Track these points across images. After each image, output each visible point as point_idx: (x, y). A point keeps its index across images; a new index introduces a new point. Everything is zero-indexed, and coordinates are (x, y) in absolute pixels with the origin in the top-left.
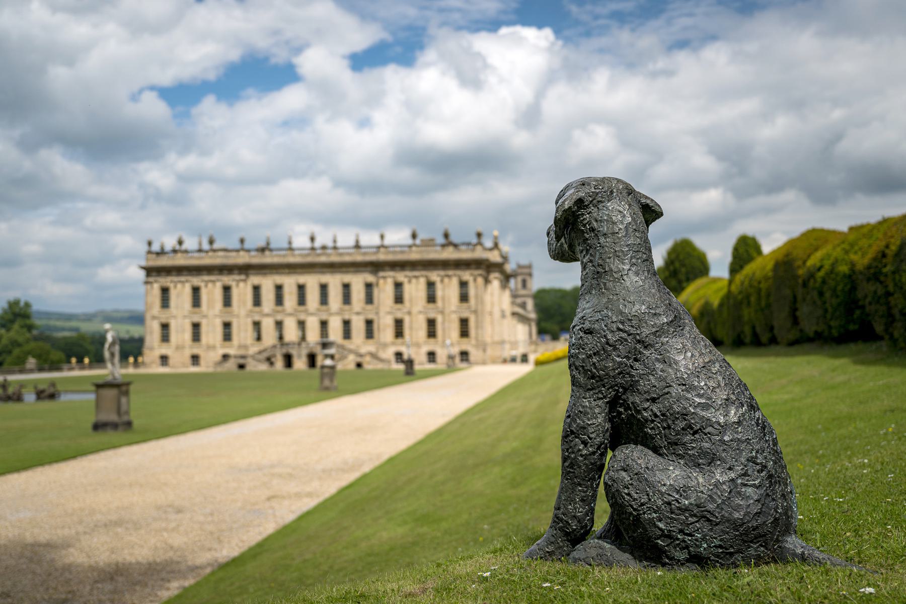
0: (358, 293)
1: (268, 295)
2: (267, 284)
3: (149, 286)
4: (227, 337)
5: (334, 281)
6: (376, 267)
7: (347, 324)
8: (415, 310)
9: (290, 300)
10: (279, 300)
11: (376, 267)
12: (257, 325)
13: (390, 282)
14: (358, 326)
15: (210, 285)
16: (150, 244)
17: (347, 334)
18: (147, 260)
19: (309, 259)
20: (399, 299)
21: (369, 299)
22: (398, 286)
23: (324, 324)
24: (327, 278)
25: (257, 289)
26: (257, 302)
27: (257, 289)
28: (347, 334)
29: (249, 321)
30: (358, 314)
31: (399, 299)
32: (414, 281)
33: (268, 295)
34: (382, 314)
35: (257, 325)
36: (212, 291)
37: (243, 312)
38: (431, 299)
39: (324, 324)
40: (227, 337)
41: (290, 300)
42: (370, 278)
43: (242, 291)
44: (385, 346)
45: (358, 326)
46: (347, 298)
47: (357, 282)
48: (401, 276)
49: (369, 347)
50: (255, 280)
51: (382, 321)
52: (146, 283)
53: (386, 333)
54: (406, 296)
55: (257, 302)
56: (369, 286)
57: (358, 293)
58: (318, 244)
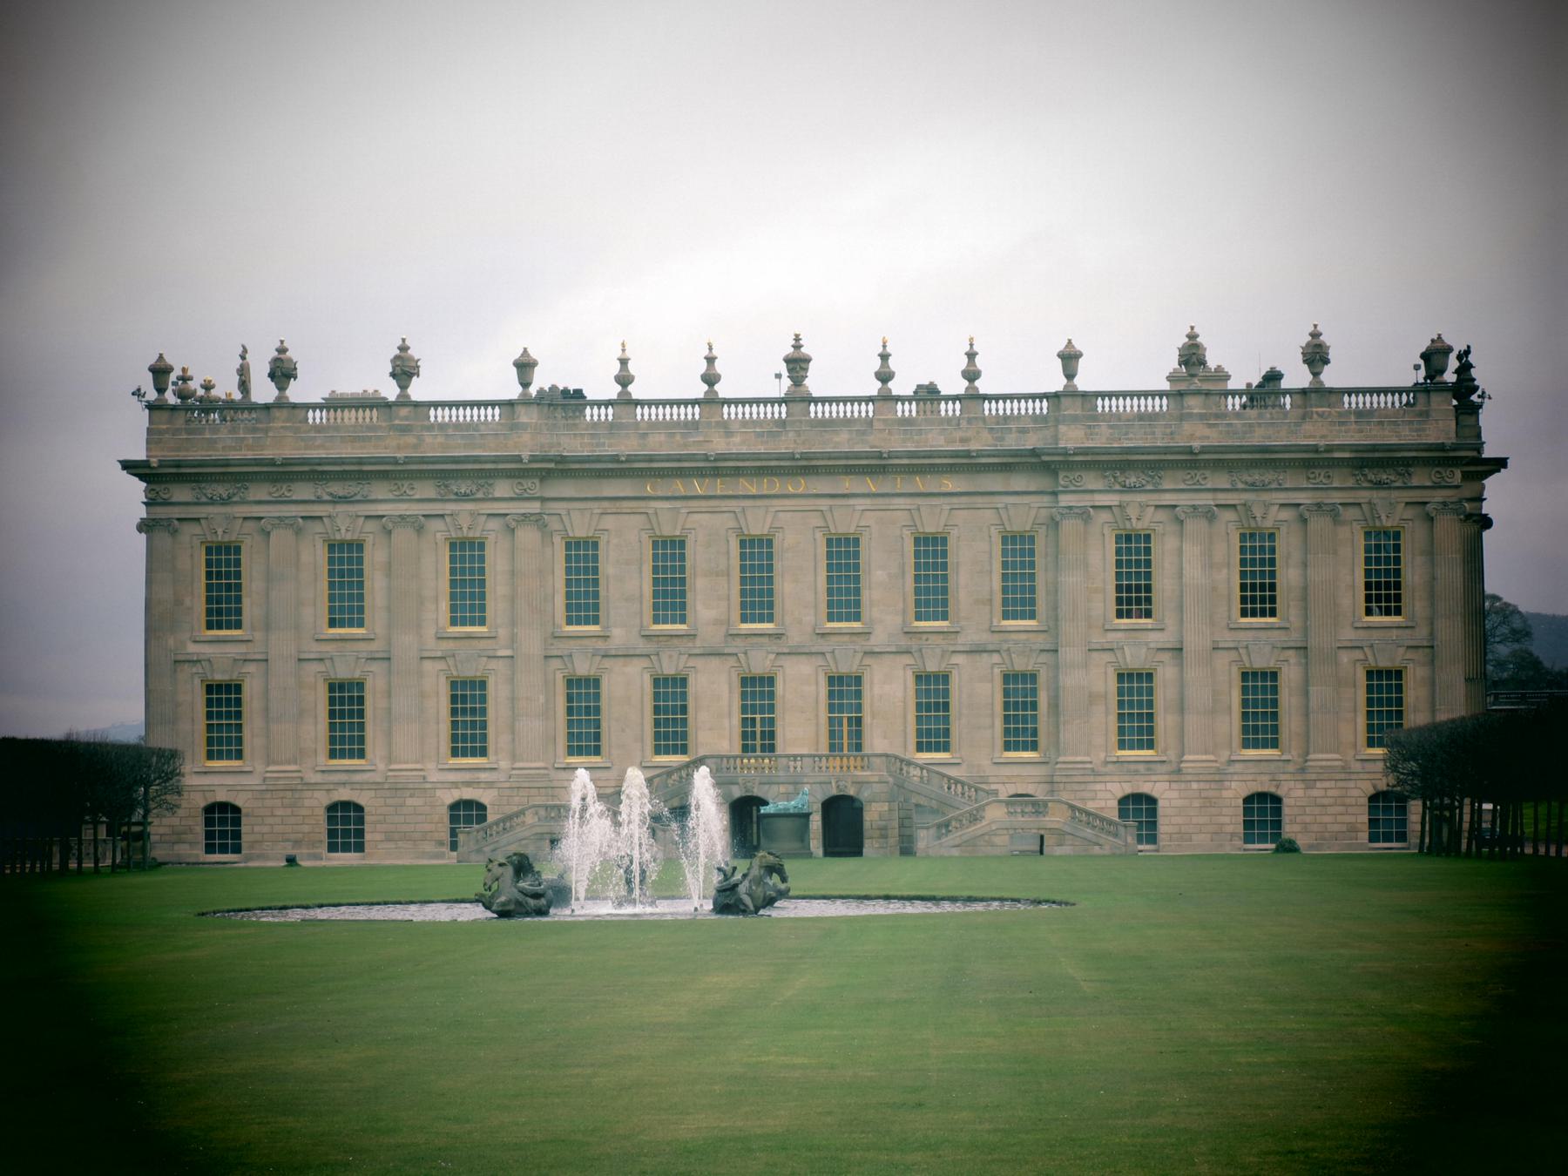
0: (975, 571)
1: (626, 579)
3: (163, 538)
4: (468, 736)
9: (712, 599)
10: (670, 595)
14: (977, 695)
15: (403, 536)
16: (160, 372)
17: (934, 729)
18: (153, 435)
19: (787, 444)
21: (1018, 598)
23: (845, 691)
26: (584, 601)
28: (934, 729)
30: (976, 651)
32: (1194, 526)
33: (626, 579)
34: (1070, 654)
37: (532, 643)
39: (845, 691)
41: (712, 599)
46: (932, 596)
48: (1142, 509)
51: (1071, 680)
52: (145, 526)
54: (1163, 584)
55: (584, 601)
56: (1018, 547)
57: (975, 571)
58: (898, 387)
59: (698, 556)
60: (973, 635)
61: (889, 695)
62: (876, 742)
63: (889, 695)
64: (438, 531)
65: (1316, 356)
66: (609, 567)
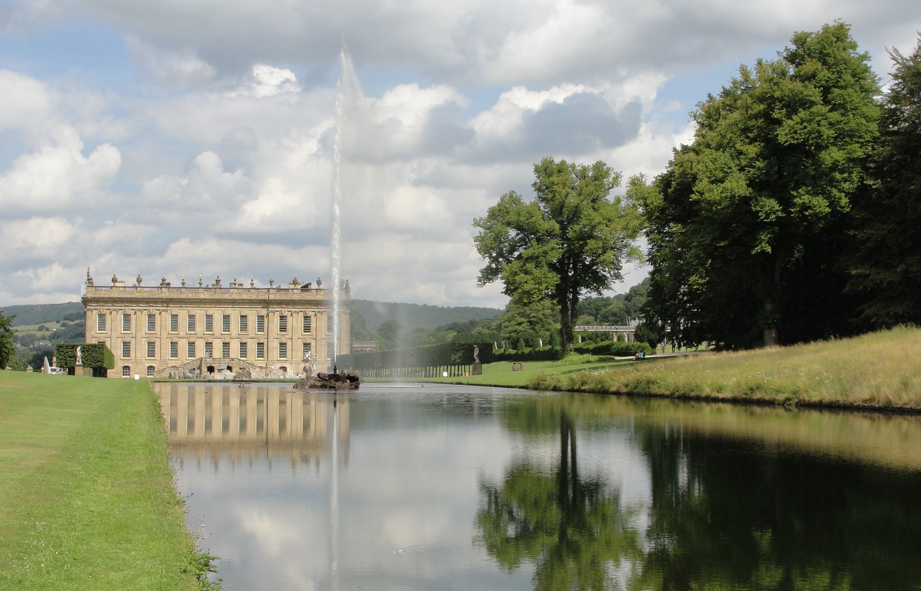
0: (253, 322)
1: (183, 322)
2: (183, 314)
4: (151, 353)
5: (235, 314)
6: (267, 303)
7: (243, 345)
8: (295, 337)
9: (200, 327)
11: (267, 303)
12: (174, 344)
13: (277, 315)
14: (252, 347)
17: (244, 352)
20: (283, 329)
21: (261, 328)
22: (283, 318)
23: (226, 345)
24: (229, 311)
25: (175, 317)
26: (175, 326)
27: (175, 317)
28: (244, 352)
29: (169, 341)
31: (283, 329)
33: (183, 322)
35: (174, 344)
36: (140, 319)
37: (164, 335)
38: (307, 329)
39: (226, 345)
40: (151, 353)
41: (200, 327)
42: (264, 312)
43: (164, 319)
44: (273, 362)
45: (252, 347)
47: (252, 314)
48: (285, 311)
49: (261, 362)
50: (175, 310)
53: (275, 353)
54: (289, 326)
55: (175, 326)
56: (261, 318)
57: (253, 322)
59: (197, 318)
60: (252, 335)
61: (235, 347)
62: (232, 355)
63: (235, 347)
64: (145, 313)
65: (319, 283)
66: (180, 320)
